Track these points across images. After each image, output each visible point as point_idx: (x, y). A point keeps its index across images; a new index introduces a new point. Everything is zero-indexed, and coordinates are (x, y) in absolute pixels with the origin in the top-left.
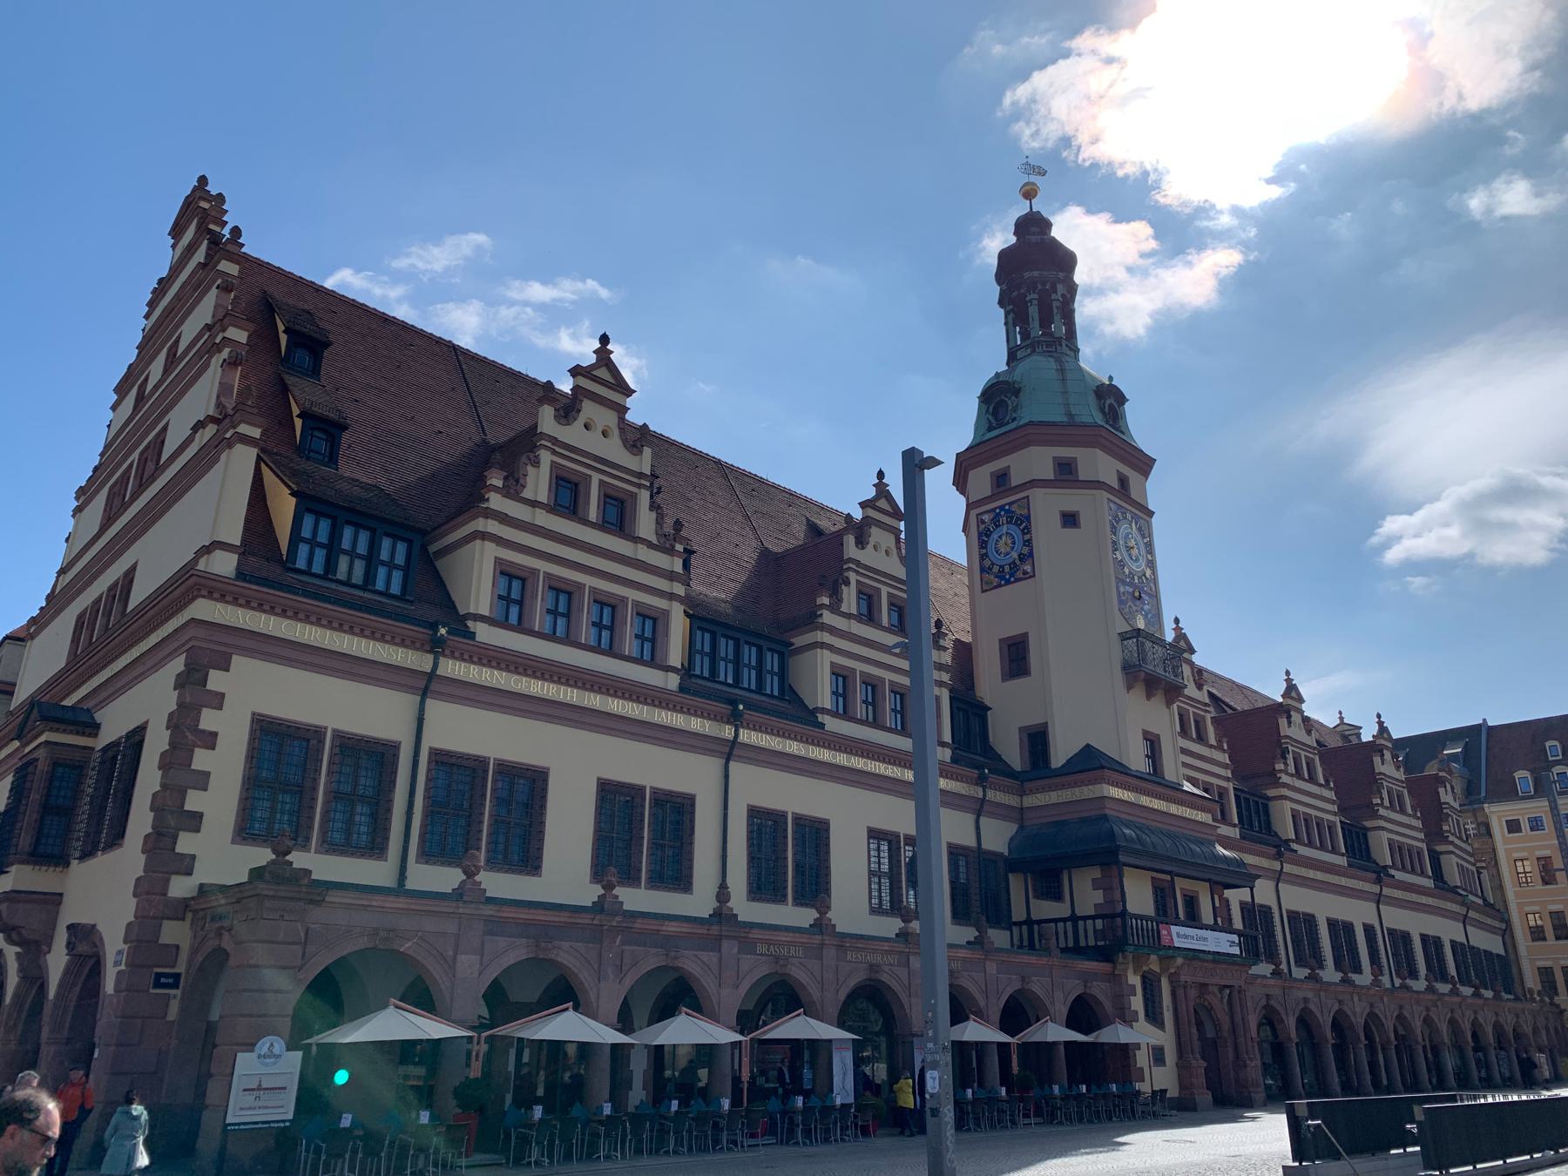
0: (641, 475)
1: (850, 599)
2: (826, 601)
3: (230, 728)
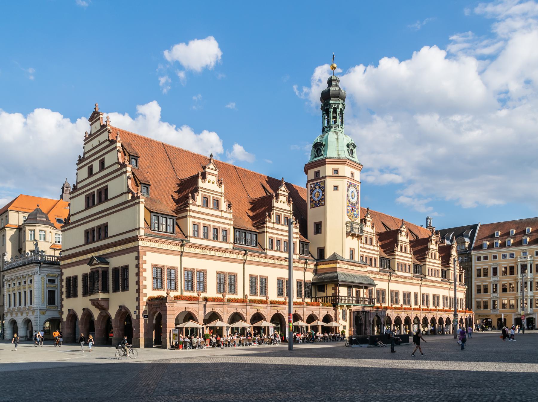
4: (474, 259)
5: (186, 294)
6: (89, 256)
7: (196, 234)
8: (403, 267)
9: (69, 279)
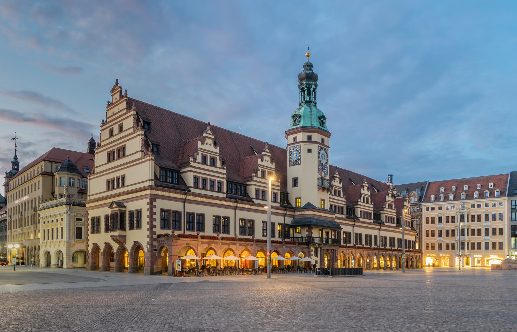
0: (217, 153)
1: (259, 174)
2: (254, 175)
3: (157, 210)
4: (424, 209)
5: (187, 233)
6: (110, 201)
7: (196, 186)
8: (364, 214)
9: (93, 219)
